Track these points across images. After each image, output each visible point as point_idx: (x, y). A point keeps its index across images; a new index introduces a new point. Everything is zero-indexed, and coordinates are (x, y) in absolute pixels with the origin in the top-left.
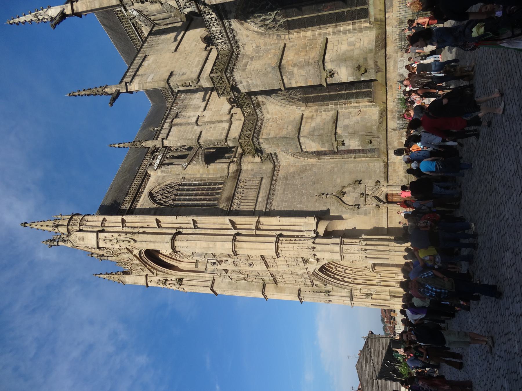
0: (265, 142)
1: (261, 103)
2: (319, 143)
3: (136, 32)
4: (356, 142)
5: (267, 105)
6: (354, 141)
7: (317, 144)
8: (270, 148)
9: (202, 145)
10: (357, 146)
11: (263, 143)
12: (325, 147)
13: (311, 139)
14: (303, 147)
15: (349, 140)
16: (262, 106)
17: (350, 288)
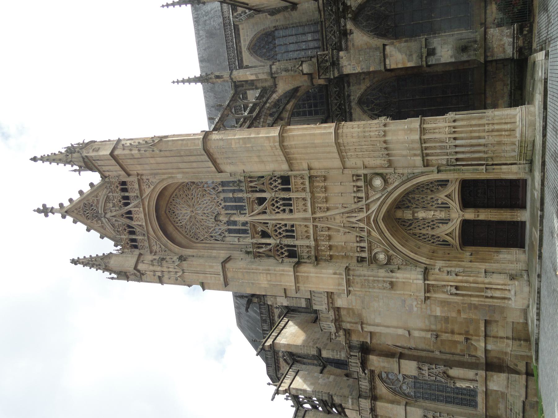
0: (345, 56)
1: (348, 31)
2: (406, 55)
3: (234, 39)
4: (448, 50)
5: (355, 34)
6: (446, 50)
7: (404, 55)
8: (349, 66)
9: (273, 72)
10: (449, 57)
11: (342, 58)
12: (412, 61)
13: (398, 48)
14: (388, 62)
15: (441, 47)
16: (348, 36)
17: (425, 266)
